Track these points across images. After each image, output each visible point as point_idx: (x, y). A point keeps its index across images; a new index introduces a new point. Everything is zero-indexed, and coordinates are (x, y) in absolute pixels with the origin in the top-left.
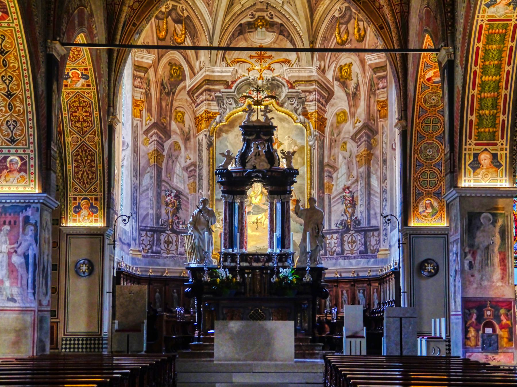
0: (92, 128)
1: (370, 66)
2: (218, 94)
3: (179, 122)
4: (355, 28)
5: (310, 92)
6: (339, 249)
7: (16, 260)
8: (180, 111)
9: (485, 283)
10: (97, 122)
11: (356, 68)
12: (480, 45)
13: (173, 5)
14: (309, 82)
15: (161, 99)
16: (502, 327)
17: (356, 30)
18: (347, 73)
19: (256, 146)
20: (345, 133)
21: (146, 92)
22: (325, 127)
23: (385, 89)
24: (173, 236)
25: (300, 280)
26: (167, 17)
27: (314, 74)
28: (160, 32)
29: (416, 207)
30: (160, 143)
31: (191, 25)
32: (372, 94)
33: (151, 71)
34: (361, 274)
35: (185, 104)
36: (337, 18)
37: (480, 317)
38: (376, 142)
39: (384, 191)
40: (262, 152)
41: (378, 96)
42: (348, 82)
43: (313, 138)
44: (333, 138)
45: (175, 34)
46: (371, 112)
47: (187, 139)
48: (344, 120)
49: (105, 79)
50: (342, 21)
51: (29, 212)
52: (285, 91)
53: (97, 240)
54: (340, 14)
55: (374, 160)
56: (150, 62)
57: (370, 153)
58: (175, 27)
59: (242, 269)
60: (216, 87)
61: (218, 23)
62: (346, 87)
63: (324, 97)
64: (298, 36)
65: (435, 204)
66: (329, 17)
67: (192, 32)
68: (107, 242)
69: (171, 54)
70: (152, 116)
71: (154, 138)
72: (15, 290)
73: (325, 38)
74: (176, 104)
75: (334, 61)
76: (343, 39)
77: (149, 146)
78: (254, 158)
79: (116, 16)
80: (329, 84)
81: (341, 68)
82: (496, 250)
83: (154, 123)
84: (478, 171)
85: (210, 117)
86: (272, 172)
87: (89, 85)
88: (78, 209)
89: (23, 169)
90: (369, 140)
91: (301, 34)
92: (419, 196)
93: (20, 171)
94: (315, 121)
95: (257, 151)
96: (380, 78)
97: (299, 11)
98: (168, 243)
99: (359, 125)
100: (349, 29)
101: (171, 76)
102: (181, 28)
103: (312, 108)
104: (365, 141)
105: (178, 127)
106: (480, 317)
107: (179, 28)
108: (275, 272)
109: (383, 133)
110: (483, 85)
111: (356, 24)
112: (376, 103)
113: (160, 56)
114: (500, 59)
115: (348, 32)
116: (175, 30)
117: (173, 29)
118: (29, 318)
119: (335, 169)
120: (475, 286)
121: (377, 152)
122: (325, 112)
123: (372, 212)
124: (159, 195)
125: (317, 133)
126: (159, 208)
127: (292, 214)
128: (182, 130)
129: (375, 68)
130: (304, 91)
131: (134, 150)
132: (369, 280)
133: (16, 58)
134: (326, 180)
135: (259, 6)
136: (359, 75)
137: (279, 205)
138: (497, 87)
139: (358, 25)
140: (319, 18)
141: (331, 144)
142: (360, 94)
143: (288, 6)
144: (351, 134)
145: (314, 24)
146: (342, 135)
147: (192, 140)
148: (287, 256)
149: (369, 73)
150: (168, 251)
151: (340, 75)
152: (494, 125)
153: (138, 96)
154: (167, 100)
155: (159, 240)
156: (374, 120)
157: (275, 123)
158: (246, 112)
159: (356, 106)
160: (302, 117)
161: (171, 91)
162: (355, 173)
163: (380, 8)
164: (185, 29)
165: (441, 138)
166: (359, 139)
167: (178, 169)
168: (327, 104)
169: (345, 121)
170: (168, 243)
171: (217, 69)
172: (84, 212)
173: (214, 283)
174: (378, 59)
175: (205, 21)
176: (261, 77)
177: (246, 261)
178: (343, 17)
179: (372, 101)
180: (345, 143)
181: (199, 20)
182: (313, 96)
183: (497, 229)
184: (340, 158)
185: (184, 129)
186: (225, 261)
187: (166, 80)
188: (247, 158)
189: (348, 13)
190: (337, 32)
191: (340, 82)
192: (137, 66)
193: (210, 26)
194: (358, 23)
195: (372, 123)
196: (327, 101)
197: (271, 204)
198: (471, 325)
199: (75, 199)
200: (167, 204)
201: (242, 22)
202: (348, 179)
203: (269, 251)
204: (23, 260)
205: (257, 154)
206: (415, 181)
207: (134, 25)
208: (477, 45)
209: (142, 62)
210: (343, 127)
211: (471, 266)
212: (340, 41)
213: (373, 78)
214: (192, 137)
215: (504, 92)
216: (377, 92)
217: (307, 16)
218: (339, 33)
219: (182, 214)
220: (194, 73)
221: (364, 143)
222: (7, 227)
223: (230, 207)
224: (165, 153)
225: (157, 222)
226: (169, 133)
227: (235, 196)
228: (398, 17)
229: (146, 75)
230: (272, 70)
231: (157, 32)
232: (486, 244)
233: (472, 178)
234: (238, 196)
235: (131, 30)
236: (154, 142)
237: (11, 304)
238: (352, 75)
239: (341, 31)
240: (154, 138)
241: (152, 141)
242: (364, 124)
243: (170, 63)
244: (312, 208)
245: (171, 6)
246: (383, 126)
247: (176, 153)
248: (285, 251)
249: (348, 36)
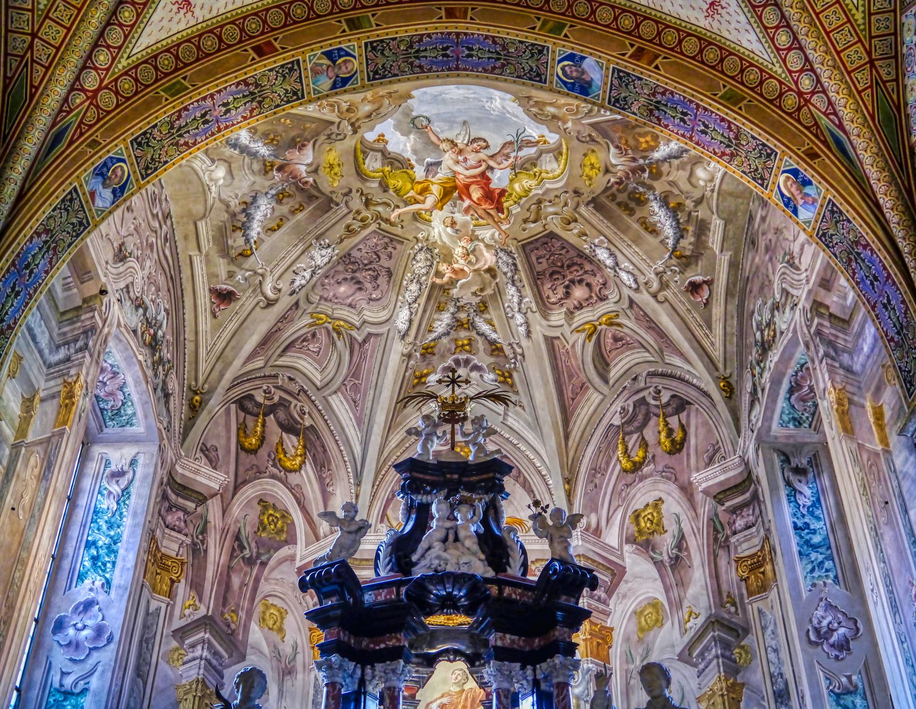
1: (706, 492)
3: (270, 629)
4: (659, 432)
8: (272, 604)
13: (281, 398)
15: (229, 568)
17: (663, 434)
18: (652, 522)
19: (445, 507)
20: (662, 651)
21: (194, 544)
22: (610, 647)
23: (754, 529)
26: (265, 415)
28: (246, 436)
30: (214, 668)
31: (318, 443)
32: (720, 547)
35: (290, 593)
36: (618, 427)
38: (747, 653)
40: (467, 528)
41: (736, 548)
42: (657, 537)
43: (583, 677)
44: (632, 667)
45: (280, 450)
46: (724, 587)
48: (657, 620)
50: (631, 428)
54: (622, 418)
55: (749, 698)
57: (733, 685)
58: (281, 437)
61: (373, 438)
62: (653, 550)
64: (537, 476)
67: (320, 456)
69: (267, 484)
70: (200, 600)
71: (198, 651)
73: (595, 470)
74: (265, 588)
75: (619, 506)
76: (637, 459)
77: (181, 668)
78: (437, 546)
79: (32, 96)
80: (613, 554)
81: (637, 516)
83: (205, 617)
86: (501, 583)
90: (728, 653)
91: (544, 473)
94: (585, 640)
95: (448, 524)
97: (540, 412)
99: (696, 624)
100: (647, 438)
101: (262, 527)
102: (296, 444)
104: (717, 657)
105: (266, 639)
107: (291, 441)
109: (764, 628)
111: (662, 424)
112: (733, 563)
113: (240, 481)
115: (644, 444)
116: (281, 442)
117: (276, 440)
121: (757, 677)
122: (608, 614)
125: (591, 665)
128: (275, 648)
129: (719, 493)
131: (138, 668)
136: (683, 517)
139: (667, 424)
140: (579, 434)
141: (628, 684)
142: (689, 556)
143: (517, 413)
144: (678, 650)
145: (570, 443)
147: (300, 676)
149: (705, 507)
151: (636, 529)
154: (245, 574)
156: (734, 604)
158: (418, 433)
159: (682, 584)
161: (258, 557)
164: (305, 447)
166: (702, 655)
168: (610, 597)
174: (725, 472)
175: (347, 442)
178: (629, 422)
179: (723, 562)
181: (336, 441)
185: (280, 647)
188: (414, 550)
189: (643, 409)
190: (619, 453)
191: (638, 544)
192: (180, 484)
193: (358, 450)
194: (666, 421)
195: (730, 613)
205: (451, 538)
209: (195, 480)
210: (655, 637)
212: (628, 466)
213: (716, 515)
214: (299, 667)
216: (733, 540)
217: (557, 423)
218: (626, 452)
221: (715, 662)
226: (241, 648)
227: (368, 670)
229: (199, 509)
231: (238, 435)
234: (379, 667)
235: (82, 153)
236: (197, 661)
238: (665, 522)
239: (630, 446)
240: (198, 651)
241: (194, 659)
242: (708, 618)
243: (261, 500)
245: (276, 399)
246: (760, 611)
249: (646, 451)
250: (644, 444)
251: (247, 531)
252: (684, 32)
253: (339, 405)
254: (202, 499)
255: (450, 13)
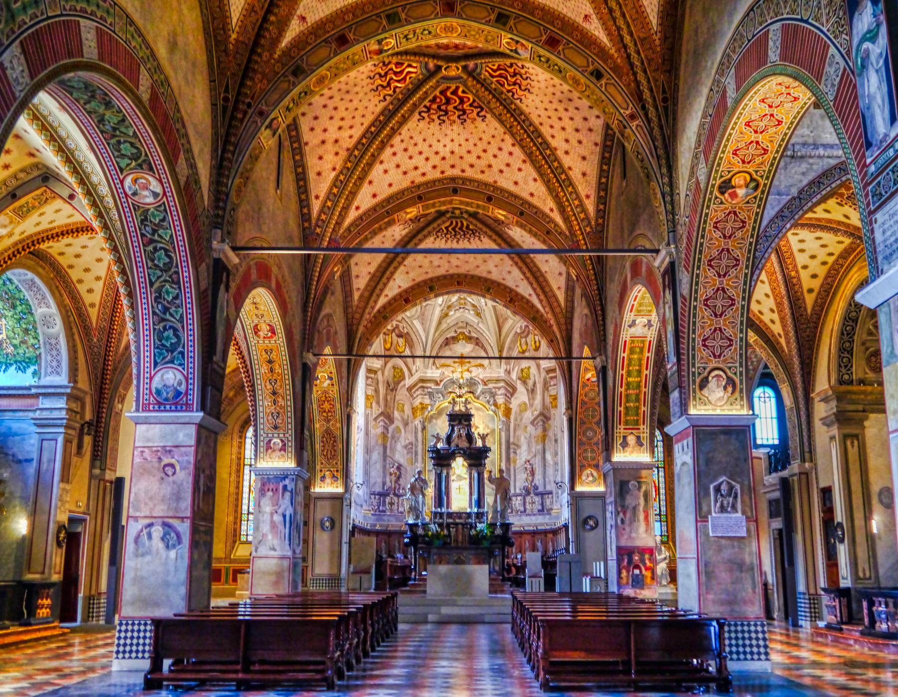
0: (334, 417)
2: (430, 390)
5: (499, 388)
6: (522, 509)
7: (278, 518)
9: (633, 535)
10: (338, 412)
11: (534, 370)
12: (625, 355)
14: (498, 381)
15: (386, 394)
16: (647, 569)
24: (395, 499)
25: (492, 532)
27: (502, 374)
29: (580, 476)
33: (380, 373)
34: (539, 528)
37: (630, 561)
39: (556, 464)
47: (406, 424)
49: (345, 380)
51: (287, 482)
52: (480, 388)
53: (338, 502)
56: (379, 366)
59: (448, 525)
60: (428, 385)
63: (509, 392)
65: (595, 474)
66: (513, 333)
68: (345, 503)
72: (276, 543)
74: (397, 398)
81: (522, 370)
82: (641, 508)
84: (626, 449)
85: (423, 407)
87: (333, 385)
88: (323, 478)
89: (283, 449)
92: (583, 468)
93: (280, 450)
96: (552, 378)
98: (391, 504)
99: (536, 413)
101: (395, 376)
103: (501, 400)
106: (630, 561)
108: (472, 526)
110: (628, 384)
114: (640, 365)
115: (527, 344)
118: (286, 563)
119: (518, 446)
120: (625, 537)
121: (551, 433)
123: (547, 480)
124: (384, 467)
126: (384, 477)
127: (486, 481)
130: (495, 388)
132: (545, 532)
133: (280, 366)
134: (512, 455)
135: (460, 325)
137: (476, 475)
138: (639, 386)
146: (524, 421)
148: (483, 514)
149: (543, 374)
150: (391, 510)
152: (637, 414)
153: (370, 392)
155: (384, 502)
157: (473, 412)
159: (534, 399)
160: (493, 407)
162: (533, 450)
163: (551, 326)
165: (598, 423)
167: (399, 447)
169: (526, 410)
170: (391, 504)
171: (429, 371)
172: (328, 480)
173: (427, 535)
176: (462, 377)
177: (451, 518)
178: (523, 332)
180: (526, 427)
182: (502, 391)
183: (642, 494)
184: (523, 439)
186: (435, 517)
187: (390, 380)
193: (424, 340)
196: (512, 395)
197: (470, 474)
198: (624, 567)
199: (321, 471)
200: (391, 474)
201: (448, 336)
202: (529, 454)
203: (469, 510)
204: (281, 518)
205: (460, 436)
206: (579, 455)
207: (368, 339)
208: (622, 355)
211: (623, 521)
215: (643, 390)
219: (401, 481)
220: (411, 375)
222: (270, 494)
223: (439, 476)
224: (389, 435)
225: (383, 488)
228: (564, 333)
230: (471, 372)
232: (633, 504)
233: (622, 455)
237: (272, 553)
244: (502, 477)
247: (397, 435)
248: (481, 510)
250: (527, 344)
251: (390, 380)
252: (523, 297)
253: (417, 323)
254: (375, 372)
255: (459, 283)
